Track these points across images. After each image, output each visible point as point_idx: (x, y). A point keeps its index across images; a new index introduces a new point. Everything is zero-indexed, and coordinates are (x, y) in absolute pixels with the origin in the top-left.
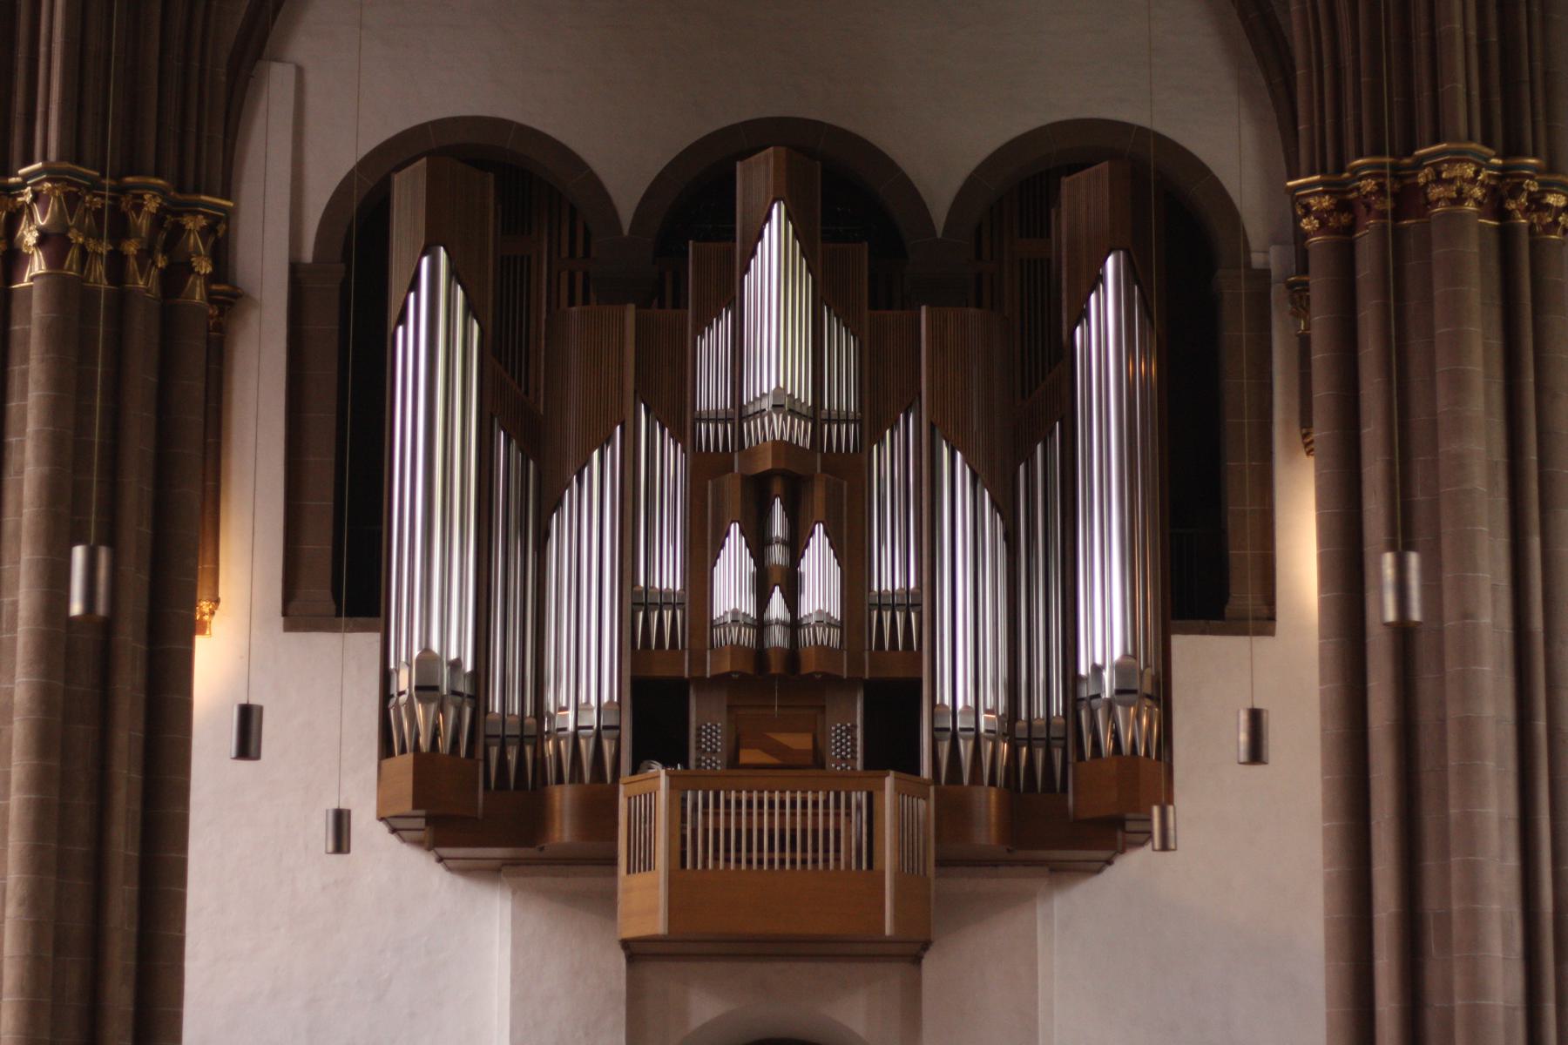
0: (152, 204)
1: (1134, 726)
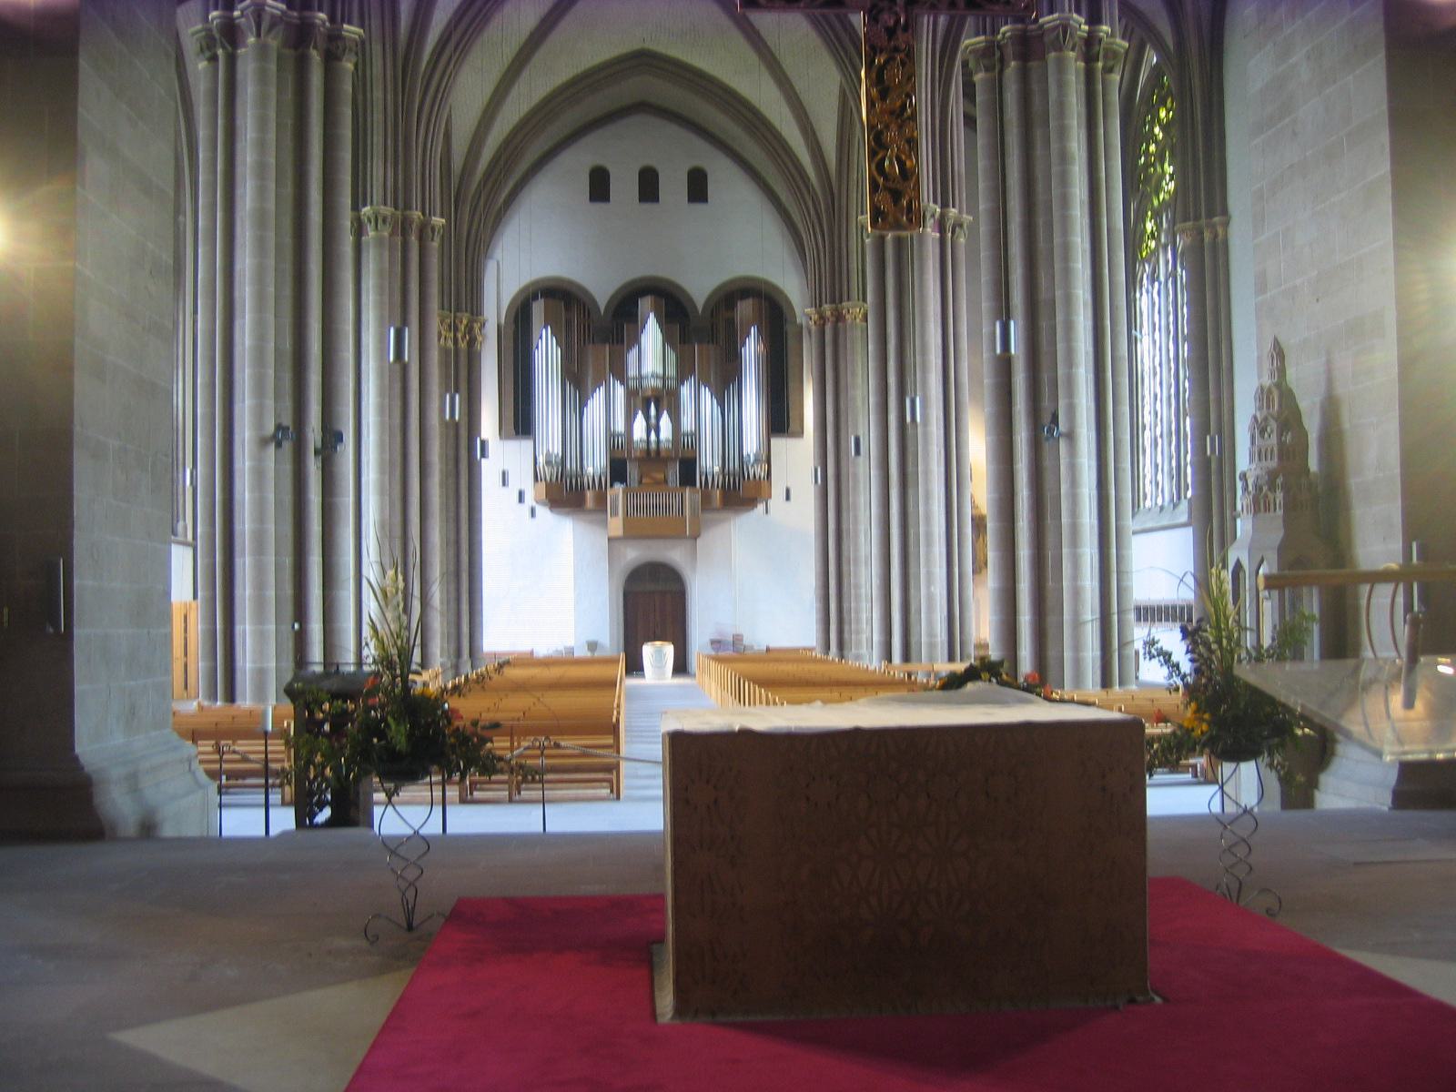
0: (465, 322)
1: (760, 471)
